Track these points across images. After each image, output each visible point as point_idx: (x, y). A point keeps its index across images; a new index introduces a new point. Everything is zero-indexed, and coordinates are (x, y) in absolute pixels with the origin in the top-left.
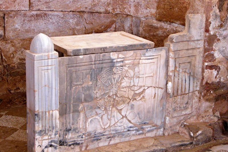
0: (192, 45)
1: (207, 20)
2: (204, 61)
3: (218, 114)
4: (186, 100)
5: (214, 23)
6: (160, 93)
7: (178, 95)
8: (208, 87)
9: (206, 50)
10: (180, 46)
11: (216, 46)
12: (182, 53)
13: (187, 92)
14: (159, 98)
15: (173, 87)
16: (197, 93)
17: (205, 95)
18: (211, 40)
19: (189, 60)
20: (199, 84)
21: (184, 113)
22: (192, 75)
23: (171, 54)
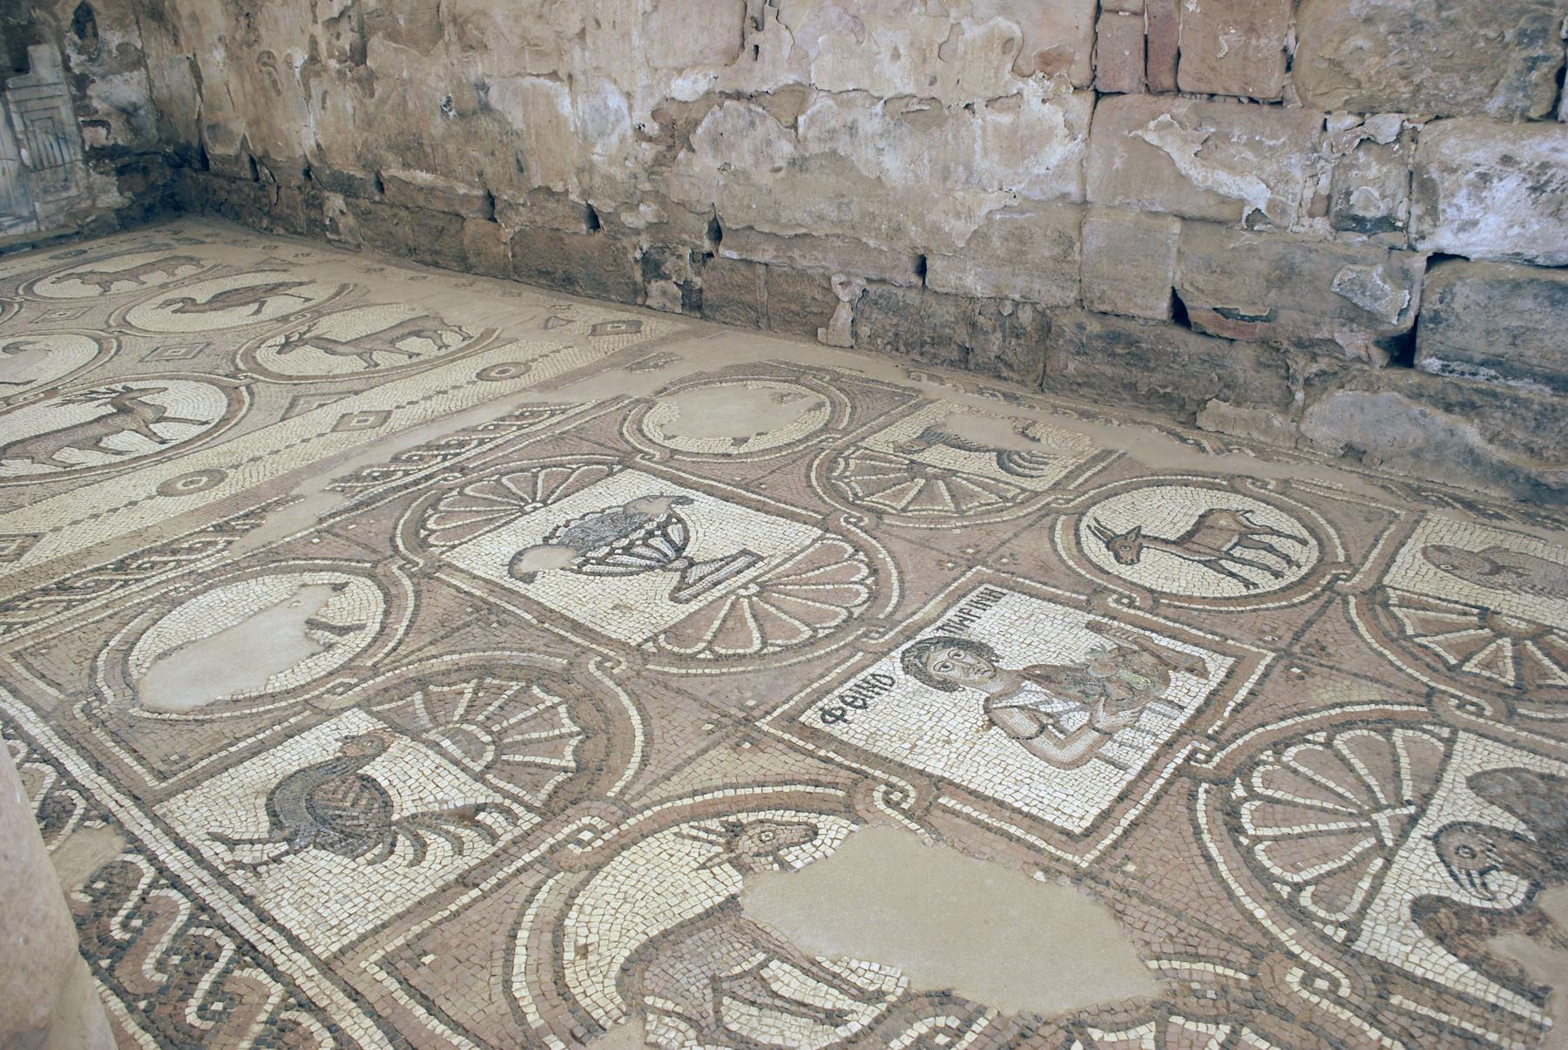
0: (46, 91)
1: (63, 53)
2: (76, 115)
3: (129, 194)
4: (62, 175)
5: (75, 59)
6: (12, 166)
7: (43, 168)
8: (96, 155)
9: (74, 99)
10: (24, 94)
11: (96, 90)
12: (30, 105)
13: (60, 162)
14: (14, 174)
15: (31, 157)
16: (80, 164)
17: (95, 167)
18: (82, 82)
19: (48, 114)
20: (78, 150)
21: (64, 195)
22: (61, 138)
23: (12, 107)
